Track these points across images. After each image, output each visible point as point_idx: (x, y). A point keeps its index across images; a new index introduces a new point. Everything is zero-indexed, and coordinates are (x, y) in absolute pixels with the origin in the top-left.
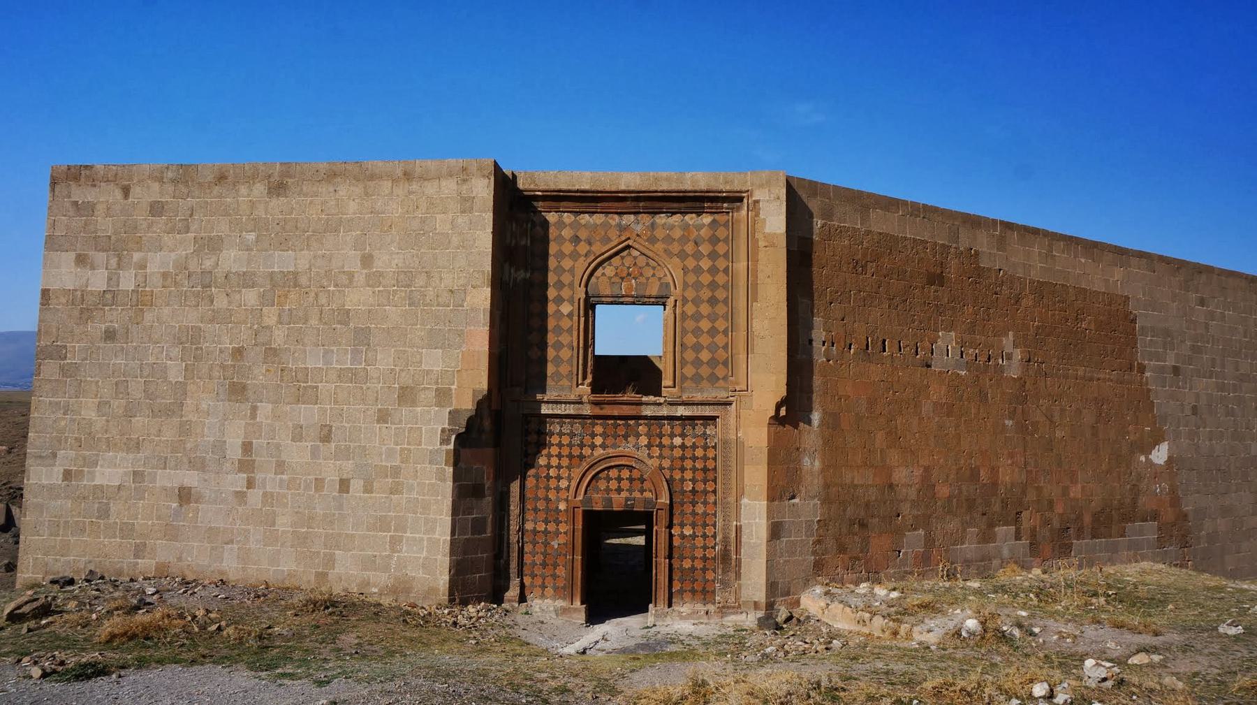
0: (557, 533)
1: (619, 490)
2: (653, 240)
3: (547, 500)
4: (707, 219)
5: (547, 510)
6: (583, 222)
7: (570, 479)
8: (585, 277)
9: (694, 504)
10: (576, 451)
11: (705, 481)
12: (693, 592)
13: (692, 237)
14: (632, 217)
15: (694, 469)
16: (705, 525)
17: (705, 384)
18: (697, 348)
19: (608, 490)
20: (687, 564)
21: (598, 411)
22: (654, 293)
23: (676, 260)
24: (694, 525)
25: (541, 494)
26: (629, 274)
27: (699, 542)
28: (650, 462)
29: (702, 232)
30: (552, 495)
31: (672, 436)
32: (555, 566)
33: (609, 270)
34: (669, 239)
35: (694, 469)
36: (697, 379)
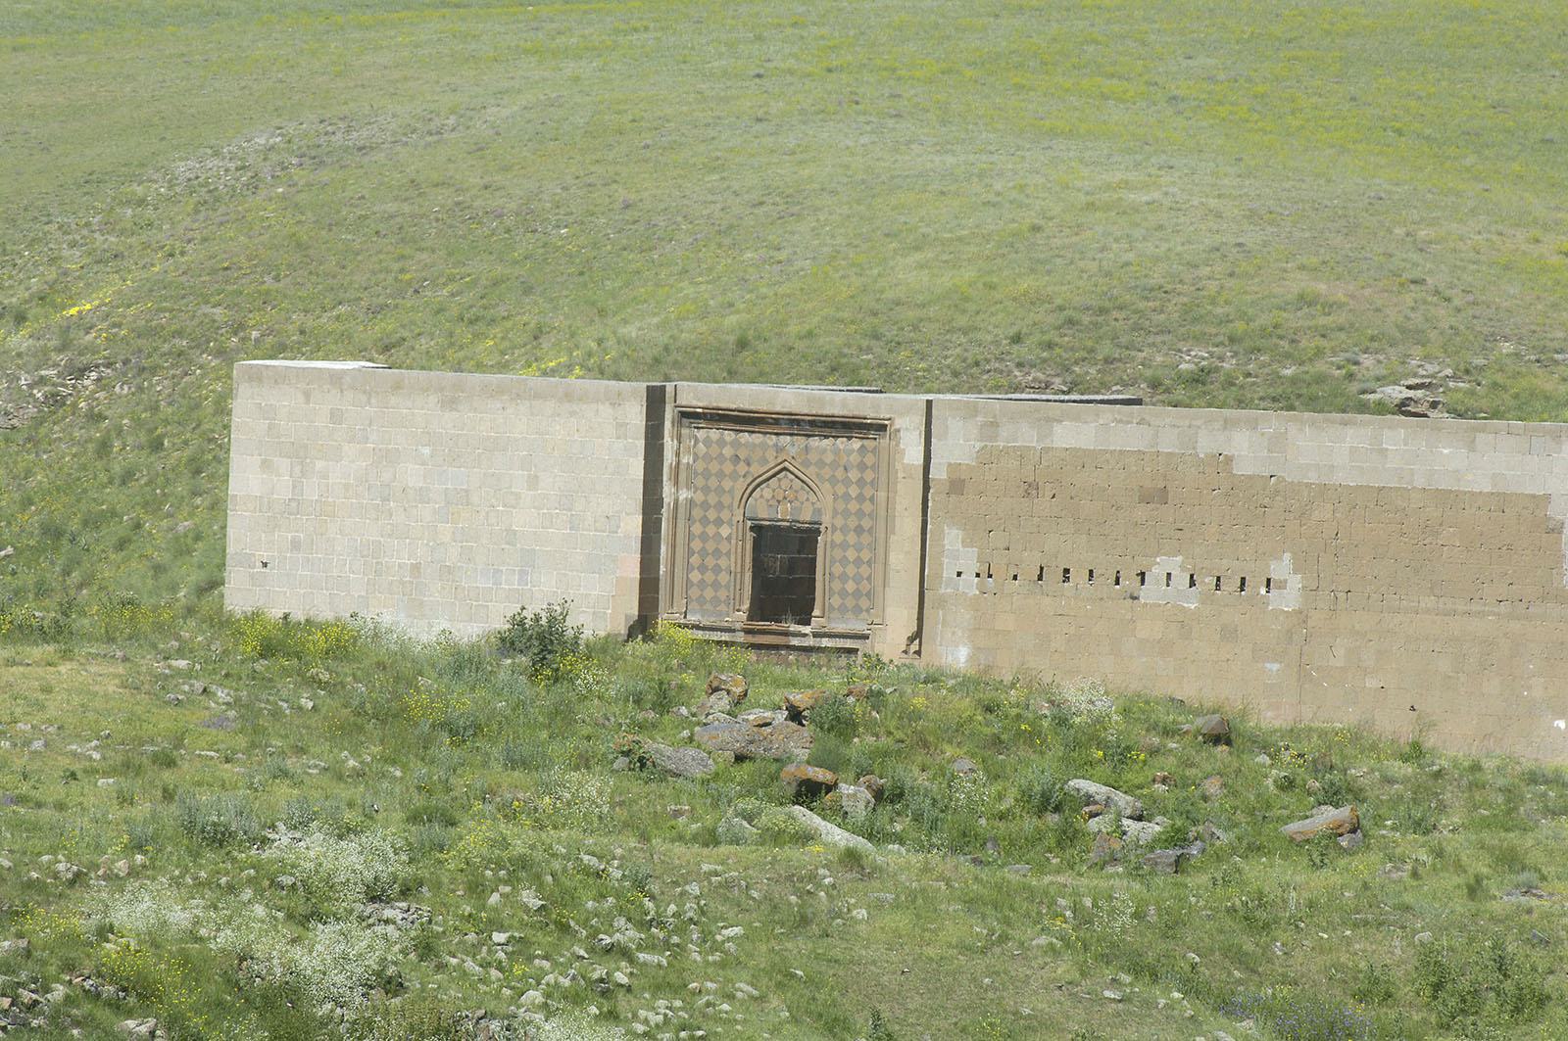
2: (807, 463)
4: (856, 444)
8: (748, 491)
17: (849, 615)
18: (844, 578)
21: (751, 639)
22: (808, 519)
23: (827, 485)
33: (766, 492)
34: (821, 464)
36: (843, 609)
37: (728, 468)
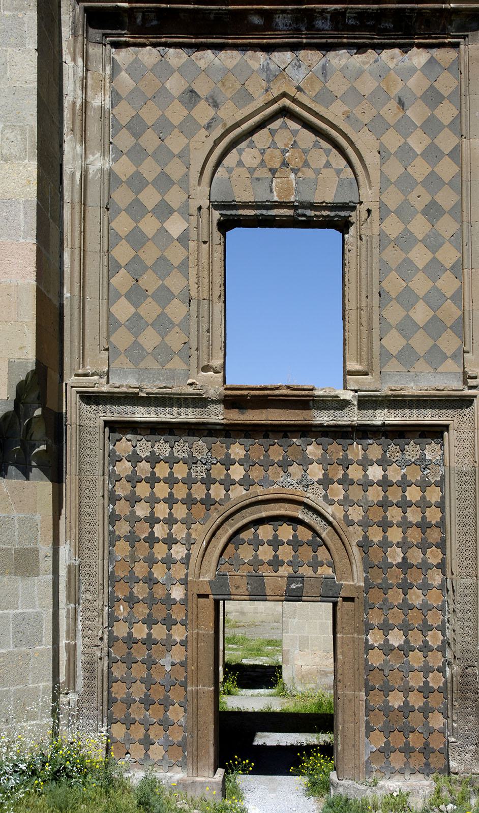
0: (168, 644)
1: (276, 563)
3: (151, 581)
5: (151, 601)
6: (202, 64)
7: (189, 543)
9: (406, 587)
10: (199, 492)
11: (424, 546)
12: (407, 750)
13: (395, 92)
14: (288, 56)
15: (405, 525)
16: (425, 628)
17: (421, 366)
18: (407, 299)
19: (256, 563)
20: (396, 700)
24: (406, 628)
25: (140, 570)
26: (285, 164)
27: (416, 659)
29: (412, 82)
30: (159, 573)
31: (365, 463)
32: (166, 704)
33: (248, 154)
35: (405, 525)
36: (407, 356)
37: (177, 113)
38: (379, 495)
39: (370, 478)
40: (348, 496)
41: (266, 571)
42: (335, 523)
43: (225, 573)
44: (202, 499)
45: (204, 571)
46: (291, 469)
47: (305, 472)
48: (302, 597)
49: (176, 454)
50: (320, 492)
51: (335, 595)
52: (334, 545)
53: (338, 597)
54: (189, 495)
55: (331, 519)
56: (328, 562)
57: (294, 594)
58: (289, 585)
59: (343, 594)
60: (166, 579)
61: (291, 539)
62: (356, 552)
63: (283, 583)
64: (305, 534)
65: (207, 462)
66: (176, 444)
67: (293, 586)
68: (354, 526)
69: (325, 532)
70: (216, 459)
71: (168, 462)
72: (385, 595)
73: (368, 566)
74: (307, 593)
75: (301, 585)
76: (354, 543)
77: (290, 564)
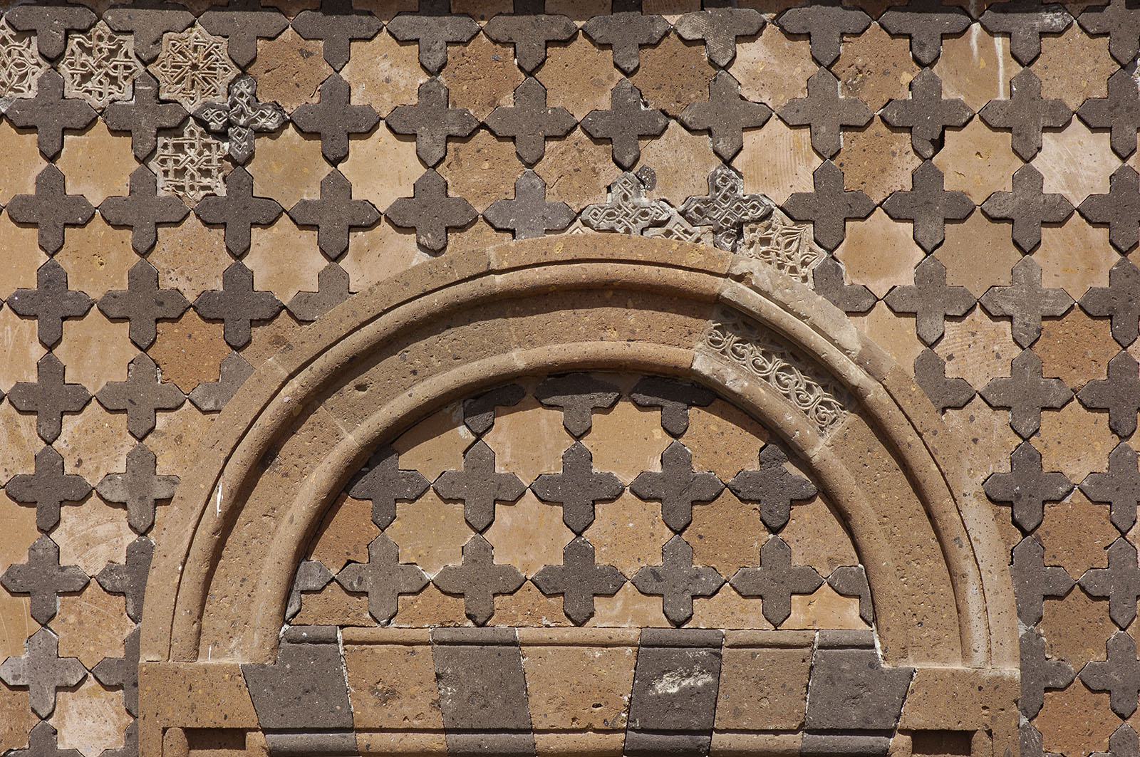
7: (144, 499)
10: (190, 263)
19: (481, 584)
28: (844, 339)
31: (1026, 122)
38: (1093, 268)
39: (1050, 187)
40: (942, 272)
41: (528, 619)
42: (875, 393)
43: (322, 632)
44: (206, 296)
45: (223, 625)
46: (653, 153)
47: (727, 163)
48: (709, 732)
49: (72, 91)
50: (798, 257)
51: (877, 724)
52: (873, 496)
53: (889, 733)
54: (144, 279)
55: (856, 375)
56: (842, 574)
57: (670, 721)
58: (643, 680)
59: (915, 718)
60: (33, 666)
61: (657, 469)
62: (981, 527)
63: (618, 673)
64: (721, 448)
65: (230, 124)
66: (73, 44)
67: (668, 686)
68: (968, 410)
69: (828, 439)
70: (277, 107)
71: (31, 129)
72: (1123, 717)
73: (1040, 593)
74: (737, 713)
75: (709, 679)
76: (971, 485)
77: (650, 584)
